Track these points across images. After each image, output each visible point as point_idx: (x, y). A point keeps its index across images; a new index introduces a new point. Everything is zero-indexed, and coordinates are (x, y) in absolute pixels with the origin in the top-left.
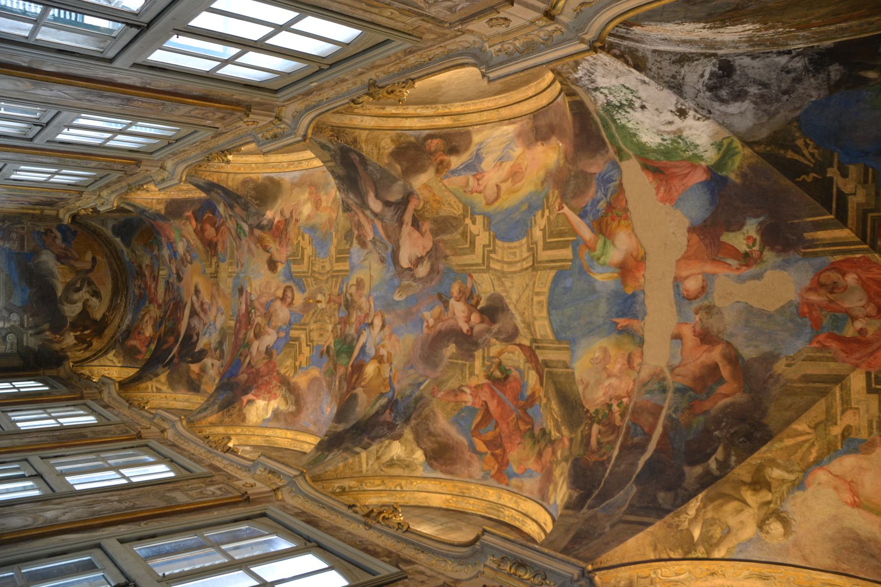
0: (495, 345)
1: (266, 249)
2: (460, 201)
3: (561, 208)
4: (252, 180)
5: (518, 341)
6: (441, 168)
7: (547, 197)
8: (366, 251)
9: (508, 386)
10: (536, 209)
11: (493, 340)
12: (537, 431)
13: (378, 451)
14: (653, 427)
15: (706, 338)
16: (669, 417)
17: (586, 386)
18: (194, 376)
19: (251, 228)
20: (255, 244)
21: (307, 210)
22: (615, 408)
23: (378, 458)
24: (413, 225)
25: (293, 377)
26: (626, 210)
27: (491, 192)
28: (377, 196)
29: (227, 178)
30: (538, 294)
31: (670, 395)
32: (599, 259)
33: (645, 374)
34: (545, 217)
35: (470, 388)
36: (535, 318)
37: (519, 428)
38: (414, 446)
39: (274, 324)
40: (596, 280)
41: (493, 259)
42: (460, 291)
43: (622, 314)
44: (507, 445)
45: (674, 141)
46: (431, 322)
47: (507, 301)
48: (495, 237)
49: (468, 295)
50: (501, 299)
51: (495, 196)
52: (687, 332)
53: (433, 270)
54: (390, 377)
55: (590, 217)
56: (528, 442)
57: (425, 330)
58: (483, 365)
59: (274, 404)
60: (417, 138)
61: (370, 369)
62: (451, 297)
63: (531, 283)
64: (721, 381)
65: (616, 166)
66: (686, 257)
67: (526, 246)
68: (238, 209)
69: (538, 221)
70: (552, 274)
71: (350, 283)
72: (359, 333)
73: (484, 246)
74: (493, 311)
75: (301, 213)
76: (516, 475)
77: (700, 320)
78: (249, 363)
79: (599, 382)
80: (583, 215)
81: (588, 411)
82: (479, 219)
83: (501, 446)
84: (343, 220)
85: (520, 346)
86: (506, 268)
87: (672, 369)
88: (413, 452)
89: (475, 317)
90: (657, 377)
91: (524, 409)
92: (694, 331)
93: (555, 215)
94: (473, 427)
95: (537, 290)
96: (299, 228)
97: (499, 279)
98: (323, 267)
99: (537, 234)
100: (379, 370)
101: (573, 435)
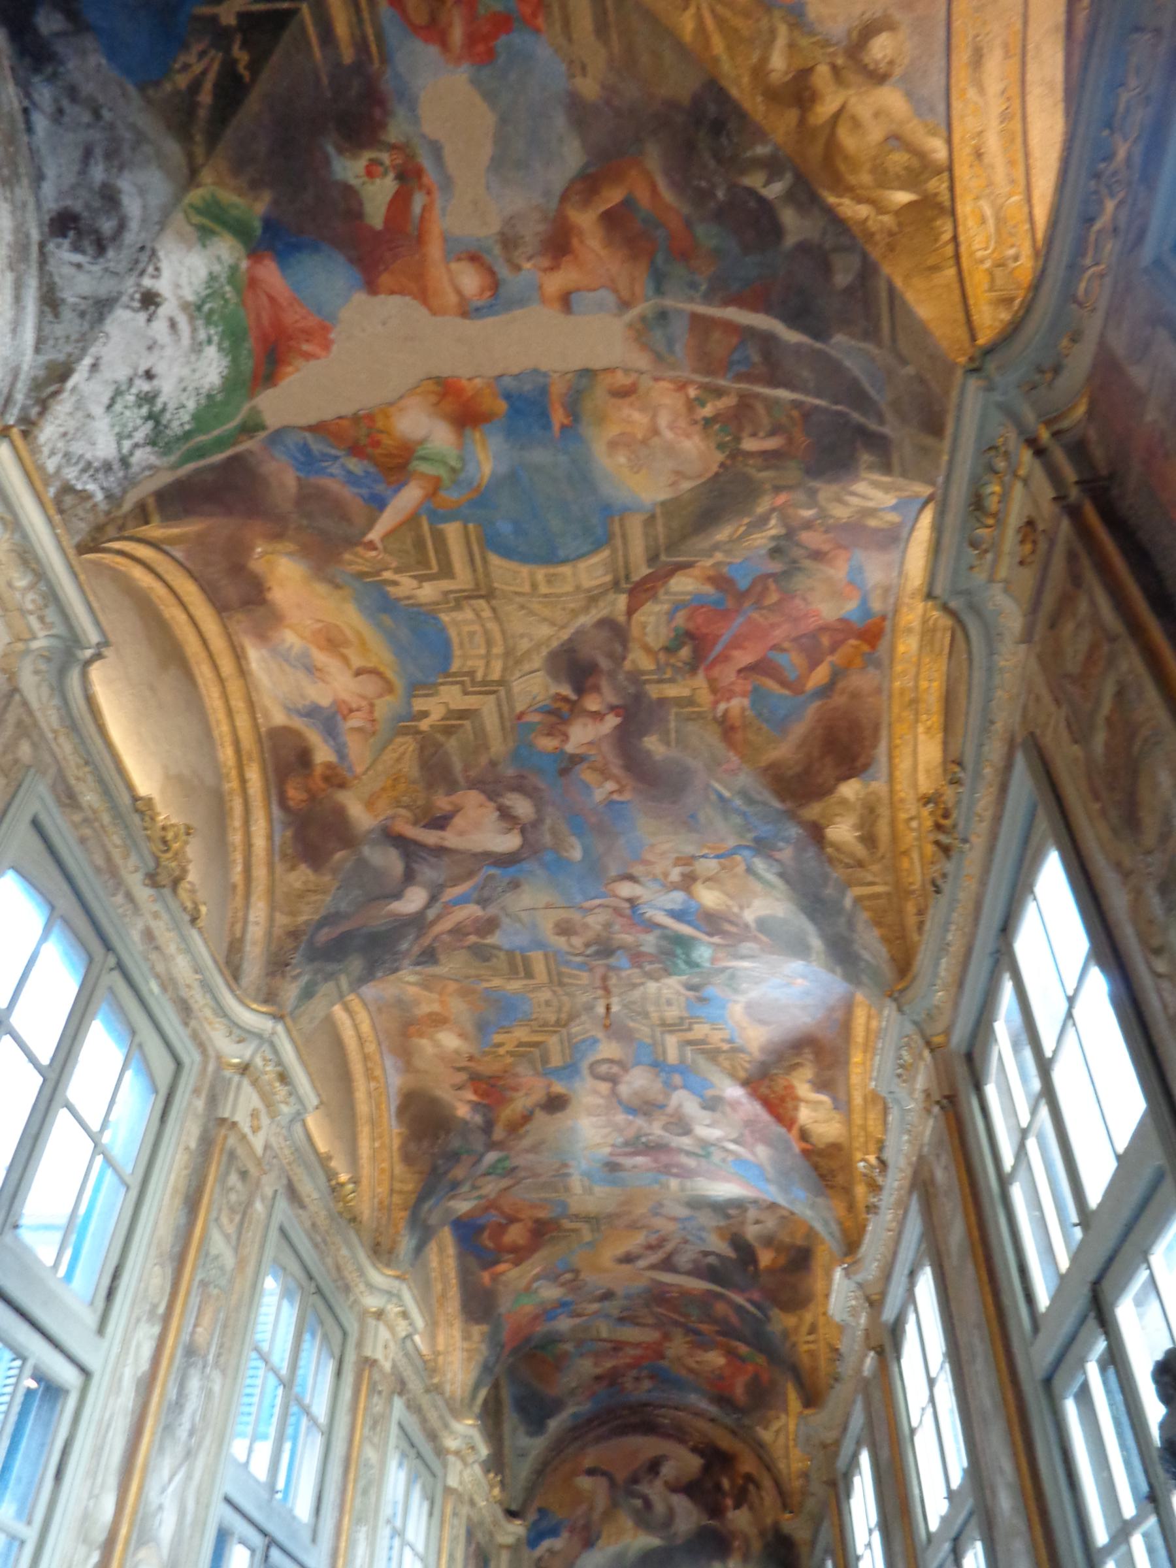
0: (633, 662)
1: (527, 1118)
2: (390, 741)
3: (371, 546)
4: (403, 1147)
5: (622, 619)
6: (336, 779)
7: (361, 575)
8: (506, 921)
9: (704, 630)
10: (385, 596)
11: (627, 665)
12: (776, 567)
13: (848, 866)
14: (730, 327)
15: (559, 245)
16: (708, 298)
17: (679, 474)
18: (782, 1261)
19: (492, 1146)
21: (450, 1041)
22: (708, 411)
23: (860, 864)
24: (442, 827)
25: (750, 1054)
26: (356, 419)
27: (370, 686)
28: (398, 895)
29: (401, 1192)
30: (534, 586)
31: (668, 302)
32: (453, 470)
33: (642, 361)
34: (396, 577)
35: (716, 703)
36: (578, 588)
37: (775, 604)
38: (833, 799)
39: (660, 1098)
40: (493, 474)
41: (485, 675)
42: (549, 734)
43: (544, 417)
44: (812, 624)
45: (208, 321)
46: (610, 786)
47: (555, 644)
48: (447, 674)
49: (553, 719)
50: (554, 656)
51: (374, 678)
52: (555, 283)
53: (520, 787)
54: (717, 857)
55: (380, 488)
56: (800, 582)
57: (627, 796)
58: (672, 681)
59: (803, 1089)
60: (286, 825)
62: (562, 752)
63: (519, 599)
64: (628, 204)
65: (277, 436)
66: (423, 295)
67: (454, 614)
68: (459, 1172)
69: (407, 593)
70: (495, 560)
71: (565, 948)
73: (466, 693)
74: (576, 668)
75: (457, 1052)
76: (864, 601)
77: (529, 259)
78: (735, 1141)
79: (670, 450)
80: (379, 504)
81: (722, 465)
82: (419, 705)
83: (814, 635)
84: (451, 965)
85: (630, 612)
86: (498, 650)
87: (625, 305)
88: (844, 802)
89: (592, 703)
90: (642, 332)
91: (742, 596)
92: (552, 269)
93: (388, 558)
94: (786, 692)
95: (527, 588)
96: (485, 1054)
97: (518, 662)
98: (548, 1003)
99: (428, 592)
100: (708, 879)
101: (768, 486)
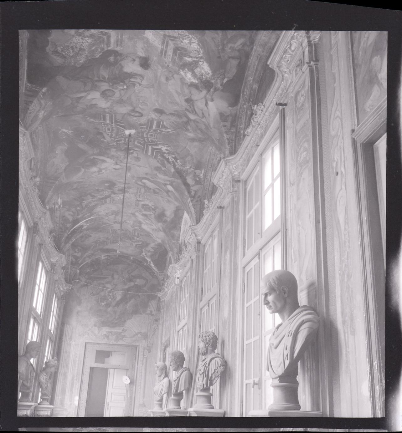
20: (177, 111)
61: (95, 169)
72: (112, 157)
78: (81, 98)
98: (152, 135)
